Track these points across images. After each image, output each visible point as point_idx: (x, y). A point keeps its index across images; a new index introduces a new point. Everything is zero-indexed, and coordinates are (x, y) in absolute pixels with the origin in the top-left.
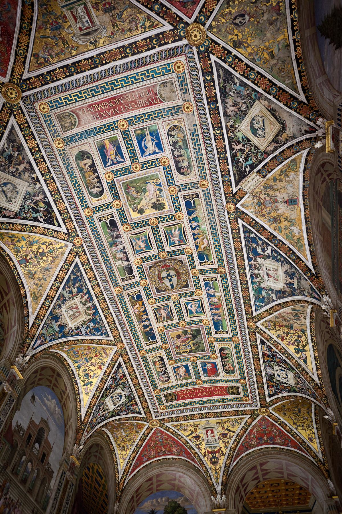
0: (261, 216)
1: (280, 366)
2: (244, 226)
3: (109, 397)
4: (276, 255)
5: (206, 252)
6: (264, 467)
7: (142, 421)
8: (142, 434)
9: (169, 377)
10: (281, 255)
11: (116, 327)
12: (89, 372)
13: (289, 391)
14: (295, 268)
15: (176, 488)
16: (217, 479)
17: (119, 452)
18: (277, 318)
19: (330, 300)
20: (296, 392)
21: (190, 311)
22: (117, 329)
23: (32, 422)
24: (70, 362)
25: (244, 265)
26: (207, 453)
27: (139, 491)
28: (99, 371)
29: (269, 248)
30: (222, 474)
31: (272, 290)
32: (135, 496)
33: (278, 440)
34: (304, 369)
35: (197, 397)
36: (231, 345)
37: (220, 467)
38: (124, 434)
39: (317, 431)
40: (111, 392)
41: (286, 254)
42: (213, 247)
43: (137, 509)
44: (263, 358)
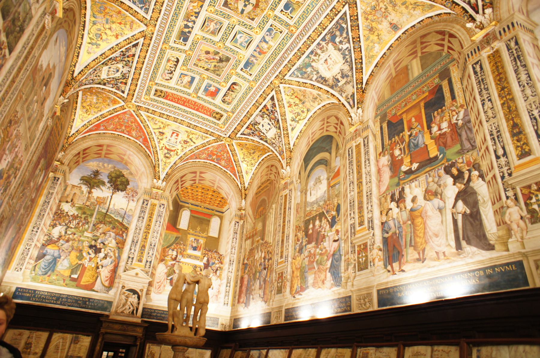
0: (365, 17)
2: (345, 13)
3: (108, 67)
4: (347, 53)
5: (295, 6)
6: (202, 175)
7: (120, 99)
8: (113, 108)
9: (171, 78)
10: (351, 57)
11: (161, 10)
12: (102, 34)
13: (261, 139)
14: (353, 74)
15: (124, 162)
16: (164, 169)
17: (81, 113)
18: (300, 91)
19: (361, 114)
21: (237, 40)
22: (160, 13)
23: (49, 65)
24: (89, 12)
25: (315, 40)
26: (164, 148)
27: (87, 151)
28: (114, 38)
29: (347, 45)
30: (169, 167)
31: (318, 73)
32: (81, 153)
33: (223, 162)
34: (288, 134)
35: (183, 105)
36: (244, 85)
37: (170, 163)
38: (95, 101)
40: (113, 63)
41: (356, 60)
42: (305, 7)
43: (81, 164)
44: (263, 108)
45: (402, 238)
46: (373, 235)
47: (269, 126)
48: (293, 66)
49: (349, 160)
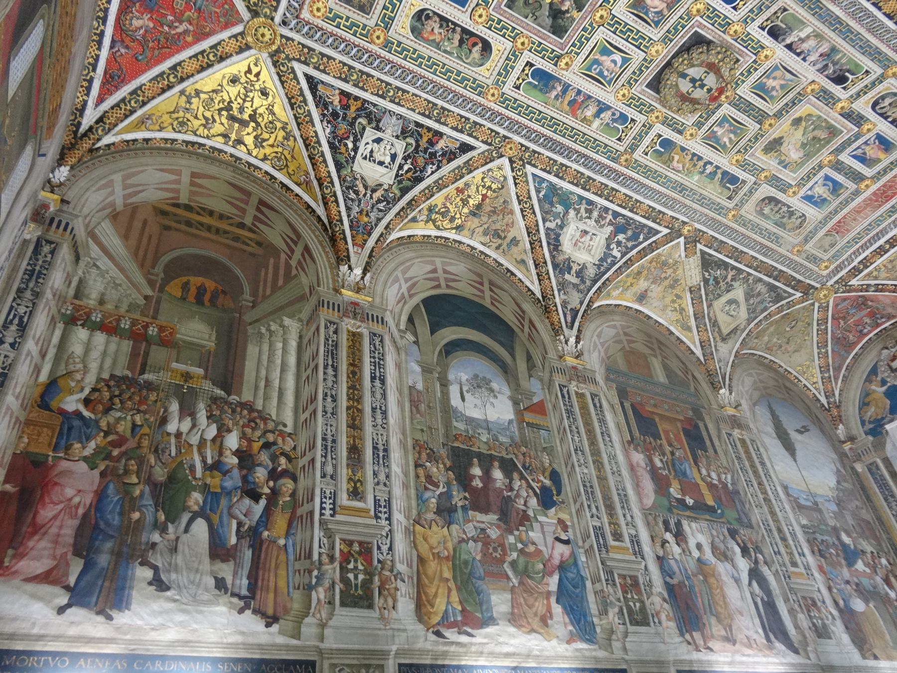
1: (405, 158)
2: (658, 232)
4: (609, 261)
5: (666, 157)
10: (608, 270)
14: (591, 288)
20: (338, 171)
25: (611, 201)
29: (619, 255)
31: (561, 227)
39: (166, 140)
41: (608, 279)
44: (429, 129)
45: (696, 596)
46: (646, 567)
47: (388, 159)
48: (557, 176)
49: (565, 405)
